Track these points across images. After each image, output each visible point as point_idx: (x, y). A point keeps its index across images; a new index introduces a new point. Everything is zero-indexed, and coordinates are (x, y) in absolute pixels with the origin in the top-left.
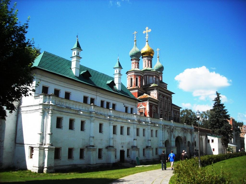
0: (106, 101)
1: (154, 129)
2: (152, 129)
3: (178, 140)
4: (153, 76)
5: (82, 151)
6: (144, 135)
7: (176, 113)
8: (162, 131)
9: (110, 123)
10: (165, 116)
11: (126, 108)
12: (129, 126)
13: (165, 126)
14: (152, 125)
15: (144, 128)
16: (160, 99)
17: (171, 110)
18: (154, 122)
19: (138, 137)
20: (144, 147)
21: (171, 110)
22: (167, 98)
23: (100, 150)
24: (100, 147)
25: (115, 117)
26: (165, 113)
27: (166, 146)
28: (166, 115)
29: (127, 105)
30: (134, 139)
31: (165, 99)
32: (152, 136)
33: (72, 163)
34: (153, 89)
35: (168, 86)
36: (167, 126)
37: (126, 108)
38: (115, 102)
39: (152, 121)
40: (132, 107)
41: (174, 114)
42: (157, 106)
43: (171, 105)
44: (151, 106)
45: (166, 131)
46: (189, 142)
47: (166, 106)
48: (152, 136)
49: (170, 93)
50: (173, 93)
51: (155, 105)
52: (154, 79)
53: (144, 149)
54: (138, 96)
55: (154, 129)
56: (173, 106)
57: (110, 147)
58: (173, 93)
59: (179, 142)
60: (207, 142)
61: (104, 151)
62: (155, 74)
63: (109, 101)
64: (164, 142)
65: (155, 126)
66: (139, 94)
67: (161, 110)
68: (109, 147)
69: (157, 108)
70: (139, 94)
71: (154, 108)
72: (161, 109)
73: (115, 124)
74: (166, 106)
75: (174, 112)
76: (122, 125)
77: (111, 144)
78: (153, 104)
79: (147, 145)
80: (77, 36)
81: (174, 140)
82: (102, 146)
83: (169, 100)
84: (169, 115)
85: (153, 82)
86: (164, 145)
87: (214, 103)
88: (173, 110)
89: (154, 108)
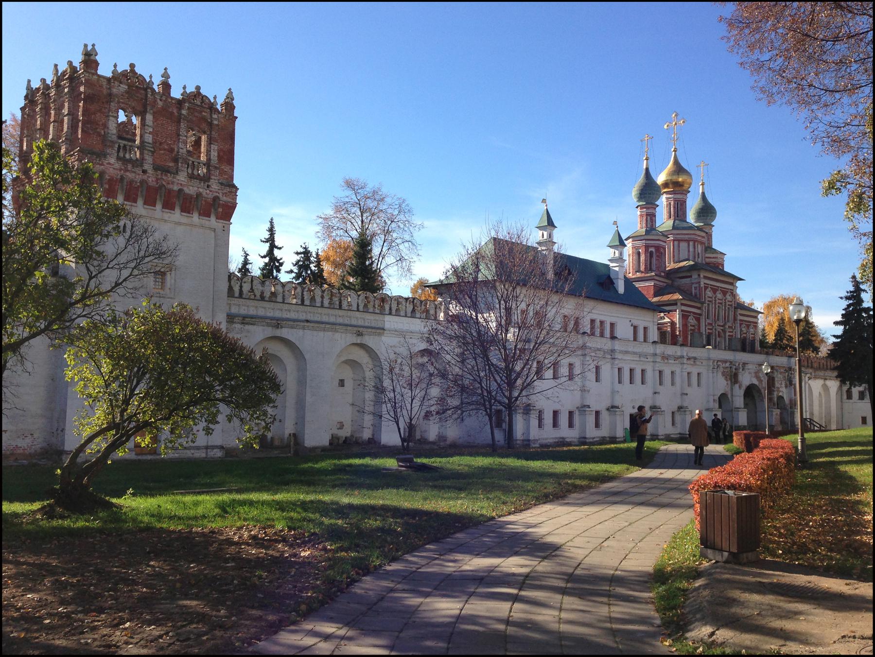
0: (598, 318)
1: (695, 371)
2: (689, 370)
3: (751, 393)
4: (688, 241)
5: (571, 413)
6: (673, 384)
7: (748, 326)
8: (711, 374)
9: (612, 364)
10: (719, 336)
11: (635, 328)
12: (644, 367)
13: (717, 364)
14: (691, 362)
15: (673, 369)
16: (708, 299)
17: (735, 319)
18: (693, 355)
19: (661, 387)
20: (675, 408)
21: (735, 319)
22: (724, 293)
23: (597, 413)
24: (598, 409)
25: (621, 352)
26: (719, 329)
27: (720, 407)
28: (722, 334)
29: (635, 323)
30: (655, 393)
31: (719, 295)
32: (689, 385)
33: (558, 436)
34: (689, 274)
35: (726, 258)
36: (725, 362)
37: (635, 328)
38: (613, 320)
39: (690, 355)
40: (646, 324)
41: (741, 330)
42: (700, 315)
43: (735, 308)
44: (685, 316)
45: (720, 374)
46: (781, 398)
47: (722, 313)
48: (689, 385)
49: (731, 281)
50: (740, 279)
51: (694, 313)
52: (691, 249)
53: (673, 413)
54: (655, 295)
55: (695, 371)
56: (739, 311)
57: (613, 407)
58: (740, 279)
59: (753, 397)
60: (845, 397)
61: (605, 417)
62: (693, 236)
63: (603, 318)
64: (717, 398)
65: (695, 364)
66: (658, 292)
67: (711, 324)
68: (612, 408)
69: (698, 320)
70: (658, 292)
71: (692, 321)
72: (708, 321)
73: (620, 366)
74: (722, 313)
75: (741, 325)
76: (633, 366)
77: (616, 404)
78: (690, 312)
79: (680, 404)
80: (544, 201)
81: (742, 392)
82: (602, 406)
83: (729, 298)
84: (728, 334)
85: (689, 255)
86: (717, 405)
87: (845, 306)
88: (741, 320)
89: (692, 321)
